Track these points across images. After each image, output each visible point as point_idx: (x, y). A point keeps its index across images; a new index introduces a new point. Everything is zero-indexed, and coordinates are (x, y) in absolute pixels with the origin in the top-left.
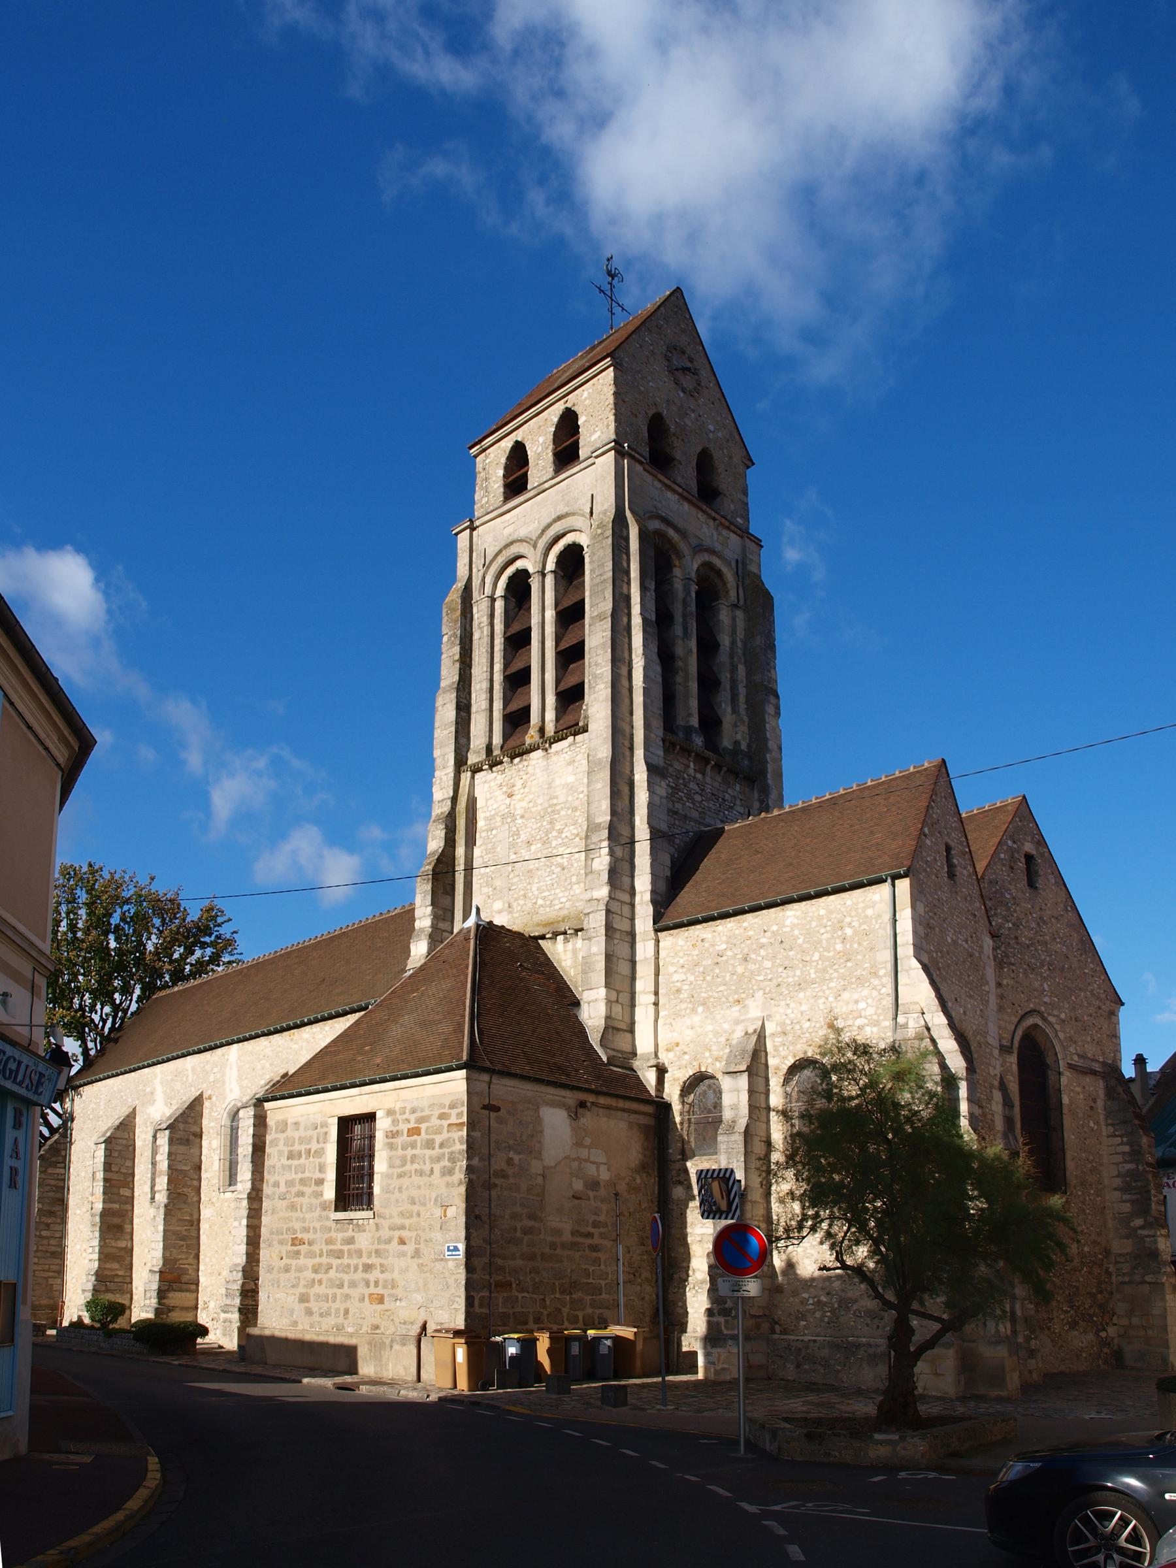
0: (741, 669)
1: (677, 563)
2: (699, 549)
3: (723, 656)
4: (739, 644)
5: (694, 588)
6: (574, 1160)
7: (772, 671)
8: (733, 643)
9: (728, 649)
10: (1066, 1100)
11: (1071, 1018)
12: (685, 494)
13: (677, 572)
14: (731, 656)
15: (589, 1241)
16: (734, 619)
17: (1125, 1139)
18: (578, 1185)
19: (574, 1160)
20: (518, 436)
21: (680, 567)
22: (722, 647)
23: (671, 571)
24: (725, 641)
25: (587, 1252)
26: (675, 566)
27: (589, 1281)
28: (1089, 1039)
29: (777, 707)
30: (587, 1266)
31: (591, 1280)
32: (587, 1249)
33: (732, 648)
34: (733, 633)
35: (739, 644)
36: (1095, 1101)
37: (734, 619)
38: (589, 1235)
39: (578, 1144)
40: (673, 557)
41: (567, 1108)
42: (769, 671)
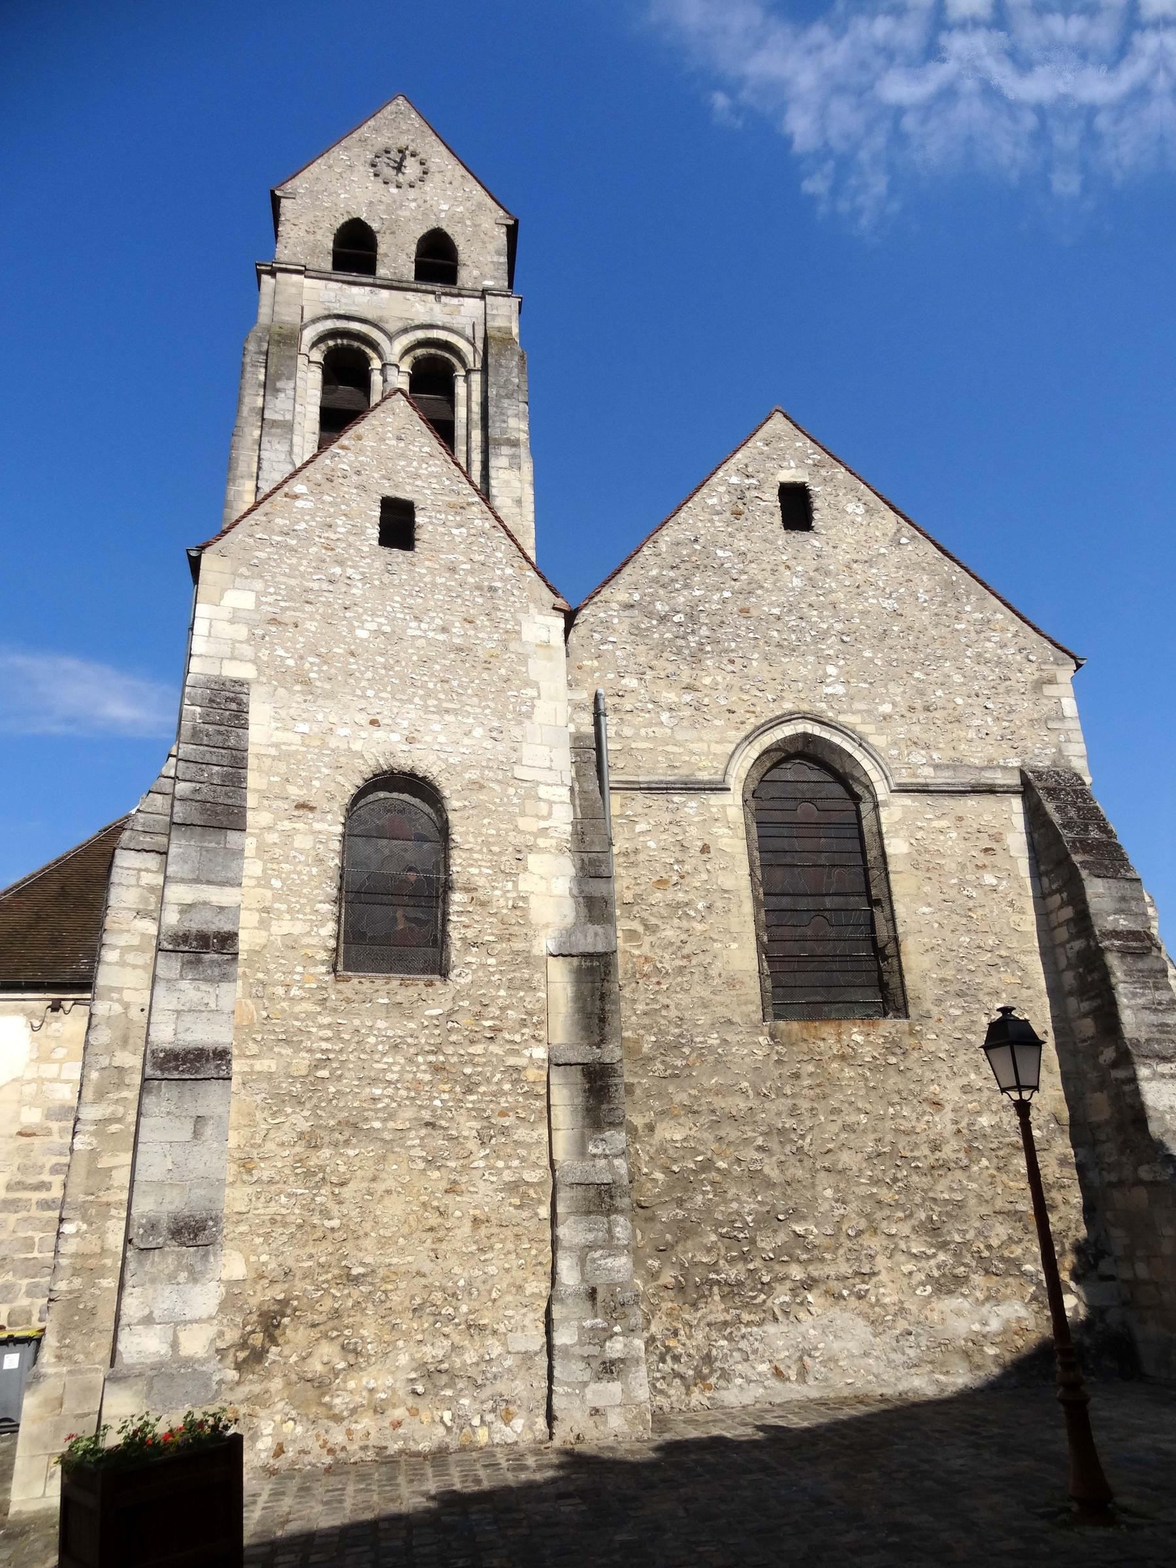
6: (29, 1082)
10: (896, 847)
11: (912, 709)
15: (43, 1195)
17: (1065, 895)
18: (32, 1117)
19: (29, 1082)
25: (35, 1212)
27: (30, 1256)
28: (972, 734)
30: (30, 1233)
31: (36, 1254)
32: (34, 1207)
36: (997, 838)
38: (44, 1186)
39: (44, 1058)
41: (30, 1015)
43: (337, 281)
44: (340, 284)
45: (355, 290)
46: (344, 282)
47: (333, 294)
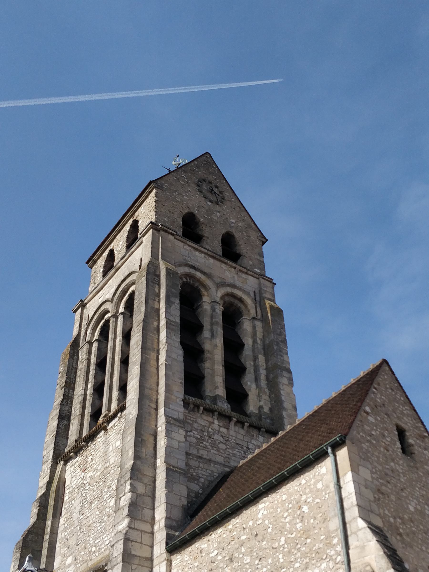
0: (261, 359)
1: (205, 293)
2: (222, 284)
3: (247, 351)
4: (259, 341)
5: (219, 309)
7: (285, 356)
8: (255, 342)
9: (251, 346)
12: (209, 253)
13: (205, 299)
14: (253, 351)
16: (254, 327)
20: (111, 247)
21: (208, 296)
22: (246, 347)
23: (201, 299)
24: (248, 341)
26: (204, 295)
29: (291, 380)
33: (253, 346)
34: (254, 334)
35: (259, 341)
37: (254, 327)
40: (202, 290)
42: (282, 356)
43: (189, 246)
44: (189, 248)
45: (197, 253)
46: (192, 247)
47: (187, 252)
